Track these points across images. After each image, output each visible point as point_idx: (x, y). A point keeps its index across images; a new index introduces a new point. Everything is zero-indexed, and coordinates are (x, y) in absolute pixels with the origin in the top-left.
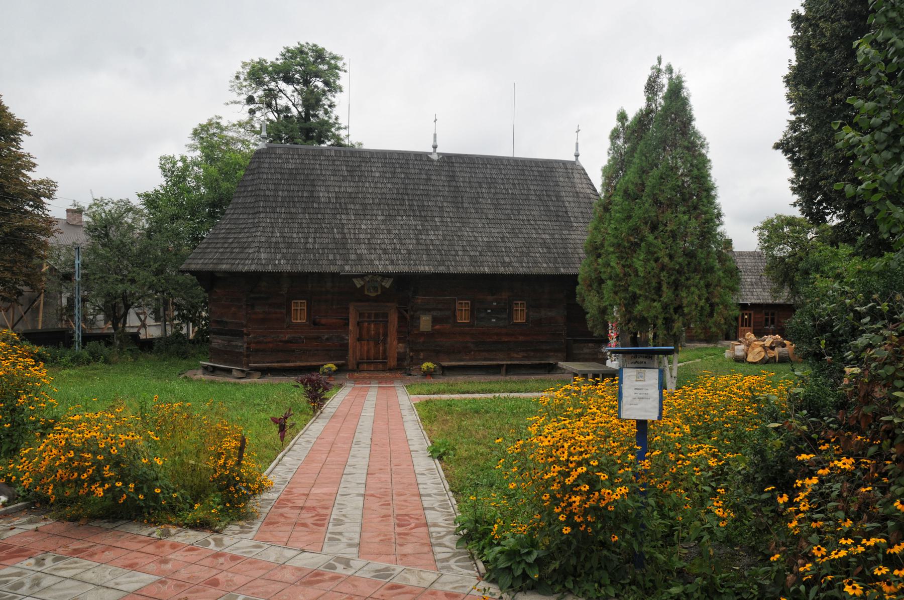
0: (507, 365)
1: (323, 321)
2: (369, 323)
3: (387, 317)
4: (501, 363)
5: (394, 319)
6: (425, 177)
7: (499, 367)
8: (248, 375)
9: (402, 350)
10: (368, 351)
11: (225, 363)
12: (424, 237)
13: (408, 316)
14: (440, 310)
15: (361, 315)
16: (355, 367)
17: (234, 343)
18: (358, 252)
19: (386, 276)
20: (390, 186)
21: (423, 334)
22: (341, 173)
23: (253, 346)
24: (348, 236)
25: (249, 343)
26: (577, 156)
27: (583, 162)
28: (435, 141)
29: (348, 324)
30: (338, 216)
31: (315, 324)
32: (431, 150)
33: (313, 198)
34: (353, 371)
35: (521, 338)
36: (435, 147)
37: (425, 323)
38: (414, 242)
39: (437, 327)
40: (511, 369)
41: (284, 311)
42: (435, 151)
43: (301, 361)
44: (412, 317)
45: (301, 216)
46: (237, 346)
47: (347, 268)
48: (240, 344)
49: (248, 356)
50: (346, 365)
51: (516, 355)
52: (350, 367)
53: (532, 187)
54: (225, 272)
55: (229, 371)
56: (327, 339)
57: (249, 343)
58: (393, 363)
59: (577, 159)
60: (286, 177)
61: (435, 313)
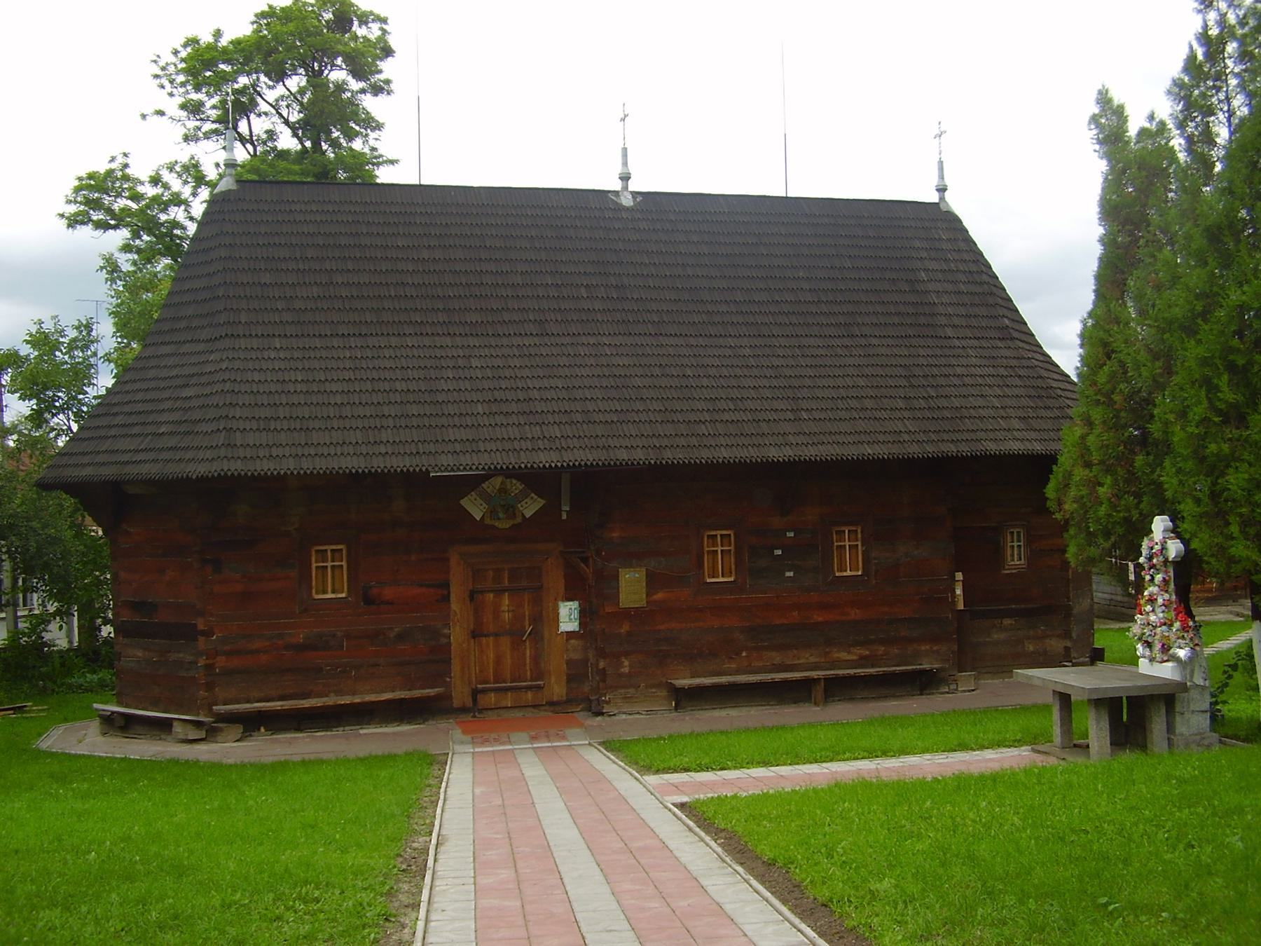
0: (828, 680)
1: (388, 593)
2: (499, 592)
4: (814, 674)
7: (808, 683)
8: (210, 733)
9: (576, 656)
10: (498, 661)
16: (469, 703)
17: (173, 657)
19: (536, 479)
21: (627, 614)
23: (221, 661)
26: (942, 190)
27: (957, 203)
28: (625, 164)
29: (446, 599)
31: (369, 600)
32: (616, 185)
34: (463, 710)
35: (855, 614)
36: (625, 178)
37: (631, 586)
39: (659, 596)
40: (839, 689)
42: (625, 188)
43: (340, 693)
47: (445, 460)
49: (209, 687)
50: (447, 697)
51: (844, 656)
54: (149, 482)
55: (164, 727)
56: (400, 637)
58: (558, 689)
59: (942, 199)
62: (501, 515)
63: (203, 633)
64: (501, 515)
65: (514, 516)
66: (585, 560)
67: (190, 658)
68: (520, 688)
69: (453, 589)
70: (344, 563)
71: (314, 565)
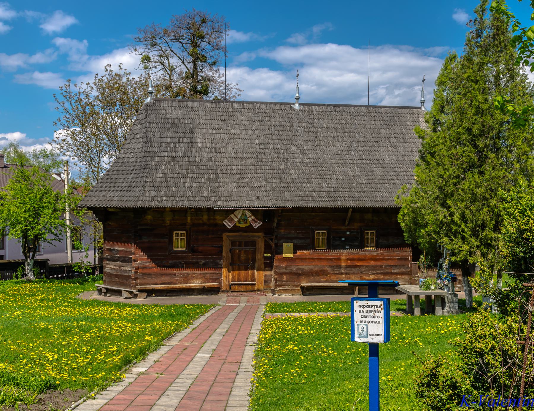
1: (201, 248)
3: (255, 245)
5: (261, 245)
6: (288, 124)
11: (116, 283)
12: (286, 176)
13: (273, 244)
14: (301, 238)
15: (233, 243)
16: (228, 288)
17: (124, 268)
18: (230, 189)
19: (254, 211)
20: (257, 132)
22: (217, 122)
24: (220, 176)
25: (137, 269)
30: (213, 159)
33: (192, 143)
38: (278, 180)
41: (167, 240)
43: (181, 283)
44: (276, 245)
45: (180, 159)
46: (126, 271)
47: (219, 203)
48: (128, 268)
52: (223, 288)
53: (383, 131)
55: (119, 293)
57: (137, 269)
58: (261, 286)
60: (169, 125)
61: (296, 241)
62: (242, 222)
63: (134, 261)
64: (242, 222)
65: (247, 223)
66: (272, 240)
67: (129, 269)
68: (247, 284)
69: (224, 248)
70: (185, 238)
71: (174, 238)
